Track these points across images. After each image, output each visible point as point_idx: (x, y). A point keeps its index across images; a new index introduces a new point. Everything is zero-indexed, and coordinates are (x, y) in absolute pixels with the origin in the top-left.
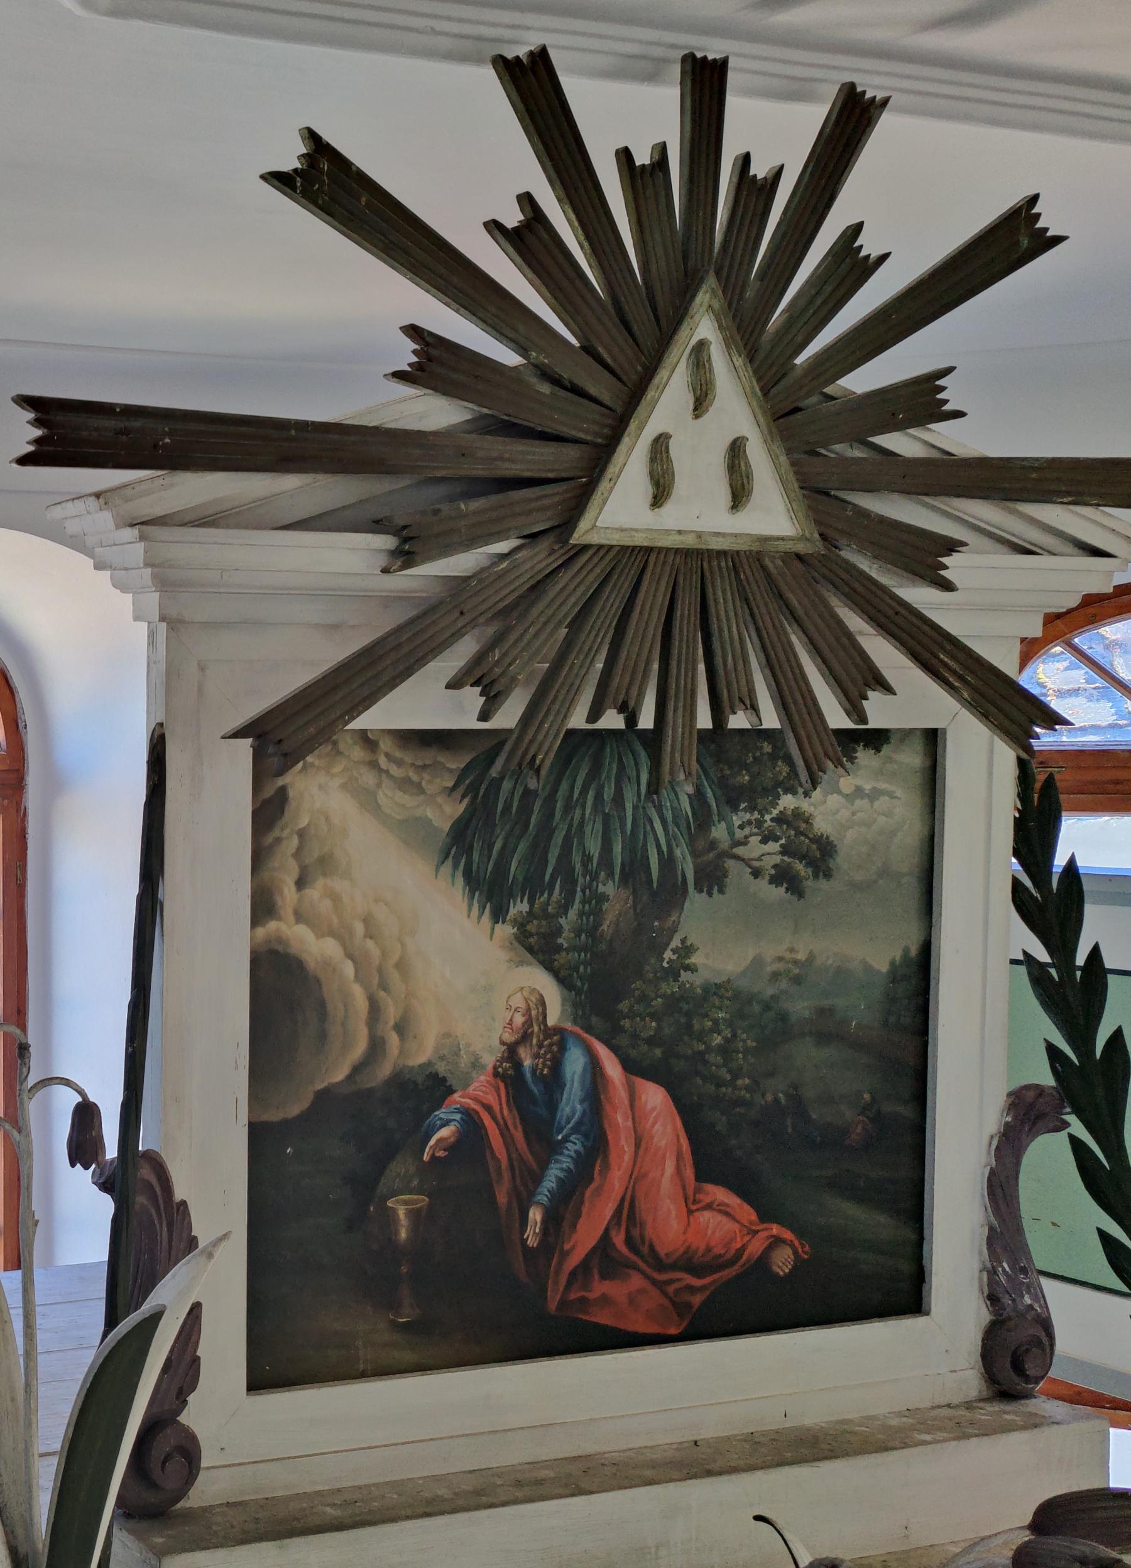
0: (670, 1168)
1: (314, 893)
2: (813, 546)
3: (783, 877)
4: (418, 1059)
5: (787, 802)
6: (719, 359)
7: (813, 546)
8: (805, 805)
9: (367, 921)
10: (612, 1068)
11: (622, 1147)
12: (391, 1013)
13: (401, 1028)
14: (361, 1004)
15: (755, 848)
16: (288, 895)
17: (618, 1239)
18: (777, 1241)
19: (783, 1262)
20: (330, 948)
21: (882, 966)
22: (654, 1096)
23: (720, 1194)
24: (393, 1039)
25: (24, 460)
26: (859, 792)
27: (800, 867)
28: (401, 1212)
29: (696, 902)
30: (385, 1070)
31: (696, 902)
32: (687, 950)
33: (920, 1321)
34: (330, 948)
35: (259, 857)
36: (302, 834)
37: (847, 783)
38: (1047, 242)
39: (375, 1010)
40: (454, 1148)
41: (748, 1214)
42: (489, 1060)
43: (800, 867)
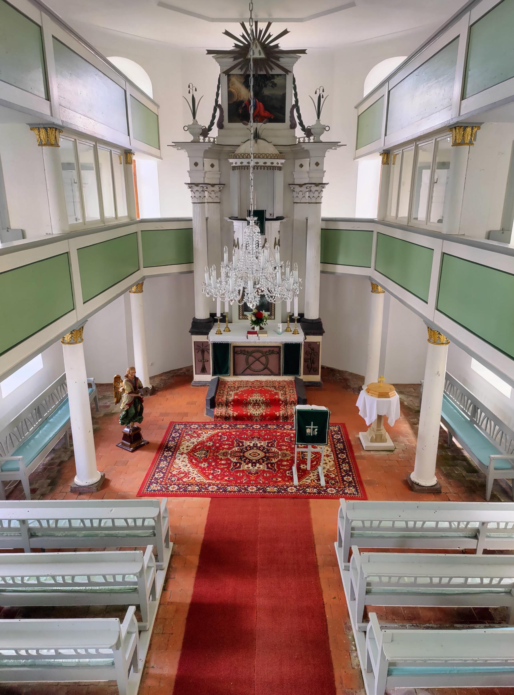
0: (262, 109)
1: (233, 86)
2: (266, 58)
3: (272, 86)
4: (241, 100)
5: (272, 80)
6: (258, 44)
7: (266, 58)
8: (274, 80)
9: (237, 89)
10: (257, 101)
11: (258, 108)
12: (239, 96)
13: (240, 97)
14: (237, 95)
15: (269, 84)
16: (231, 86)
17: (258, 114)
18: (272, 116)
19: (272, 118)
20: (234, 90)
21: (282, 94)
22: (261, 104)
23: (266, 111)
24: (239, 98)
25: (206, 54)
26: (279, 80)
27: (273, 85)
28: (240, 111)
29: (264, 88)
30: (239, 100)
31: (264, 88)
32: (263, 92)
33: (283, 124)
34: (234, 90)
35: (228, 84)
36: (232, 82)
37: (278, 79)
38: (288, 32)
39: (238, 95)
40: (245, 106)
41: (269, 113)
42: (247, 100)
43: (273, 85)
